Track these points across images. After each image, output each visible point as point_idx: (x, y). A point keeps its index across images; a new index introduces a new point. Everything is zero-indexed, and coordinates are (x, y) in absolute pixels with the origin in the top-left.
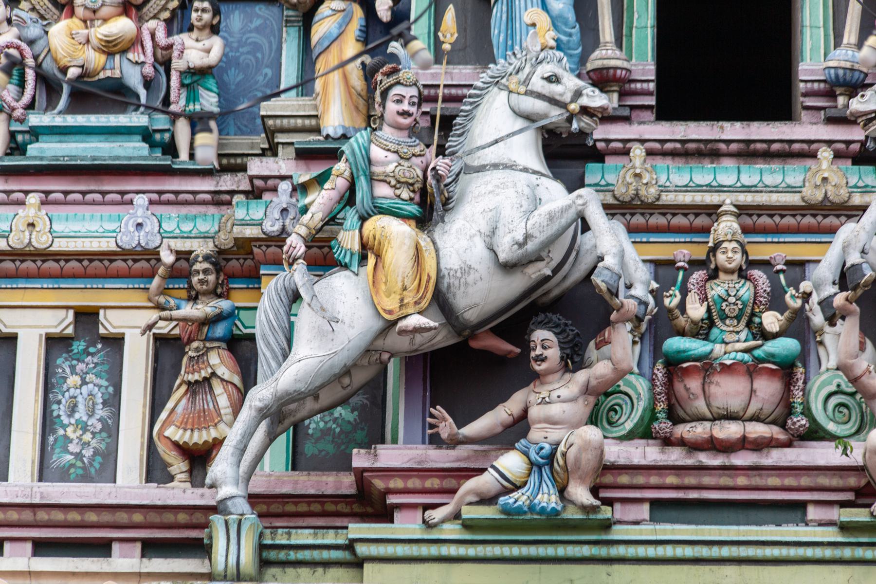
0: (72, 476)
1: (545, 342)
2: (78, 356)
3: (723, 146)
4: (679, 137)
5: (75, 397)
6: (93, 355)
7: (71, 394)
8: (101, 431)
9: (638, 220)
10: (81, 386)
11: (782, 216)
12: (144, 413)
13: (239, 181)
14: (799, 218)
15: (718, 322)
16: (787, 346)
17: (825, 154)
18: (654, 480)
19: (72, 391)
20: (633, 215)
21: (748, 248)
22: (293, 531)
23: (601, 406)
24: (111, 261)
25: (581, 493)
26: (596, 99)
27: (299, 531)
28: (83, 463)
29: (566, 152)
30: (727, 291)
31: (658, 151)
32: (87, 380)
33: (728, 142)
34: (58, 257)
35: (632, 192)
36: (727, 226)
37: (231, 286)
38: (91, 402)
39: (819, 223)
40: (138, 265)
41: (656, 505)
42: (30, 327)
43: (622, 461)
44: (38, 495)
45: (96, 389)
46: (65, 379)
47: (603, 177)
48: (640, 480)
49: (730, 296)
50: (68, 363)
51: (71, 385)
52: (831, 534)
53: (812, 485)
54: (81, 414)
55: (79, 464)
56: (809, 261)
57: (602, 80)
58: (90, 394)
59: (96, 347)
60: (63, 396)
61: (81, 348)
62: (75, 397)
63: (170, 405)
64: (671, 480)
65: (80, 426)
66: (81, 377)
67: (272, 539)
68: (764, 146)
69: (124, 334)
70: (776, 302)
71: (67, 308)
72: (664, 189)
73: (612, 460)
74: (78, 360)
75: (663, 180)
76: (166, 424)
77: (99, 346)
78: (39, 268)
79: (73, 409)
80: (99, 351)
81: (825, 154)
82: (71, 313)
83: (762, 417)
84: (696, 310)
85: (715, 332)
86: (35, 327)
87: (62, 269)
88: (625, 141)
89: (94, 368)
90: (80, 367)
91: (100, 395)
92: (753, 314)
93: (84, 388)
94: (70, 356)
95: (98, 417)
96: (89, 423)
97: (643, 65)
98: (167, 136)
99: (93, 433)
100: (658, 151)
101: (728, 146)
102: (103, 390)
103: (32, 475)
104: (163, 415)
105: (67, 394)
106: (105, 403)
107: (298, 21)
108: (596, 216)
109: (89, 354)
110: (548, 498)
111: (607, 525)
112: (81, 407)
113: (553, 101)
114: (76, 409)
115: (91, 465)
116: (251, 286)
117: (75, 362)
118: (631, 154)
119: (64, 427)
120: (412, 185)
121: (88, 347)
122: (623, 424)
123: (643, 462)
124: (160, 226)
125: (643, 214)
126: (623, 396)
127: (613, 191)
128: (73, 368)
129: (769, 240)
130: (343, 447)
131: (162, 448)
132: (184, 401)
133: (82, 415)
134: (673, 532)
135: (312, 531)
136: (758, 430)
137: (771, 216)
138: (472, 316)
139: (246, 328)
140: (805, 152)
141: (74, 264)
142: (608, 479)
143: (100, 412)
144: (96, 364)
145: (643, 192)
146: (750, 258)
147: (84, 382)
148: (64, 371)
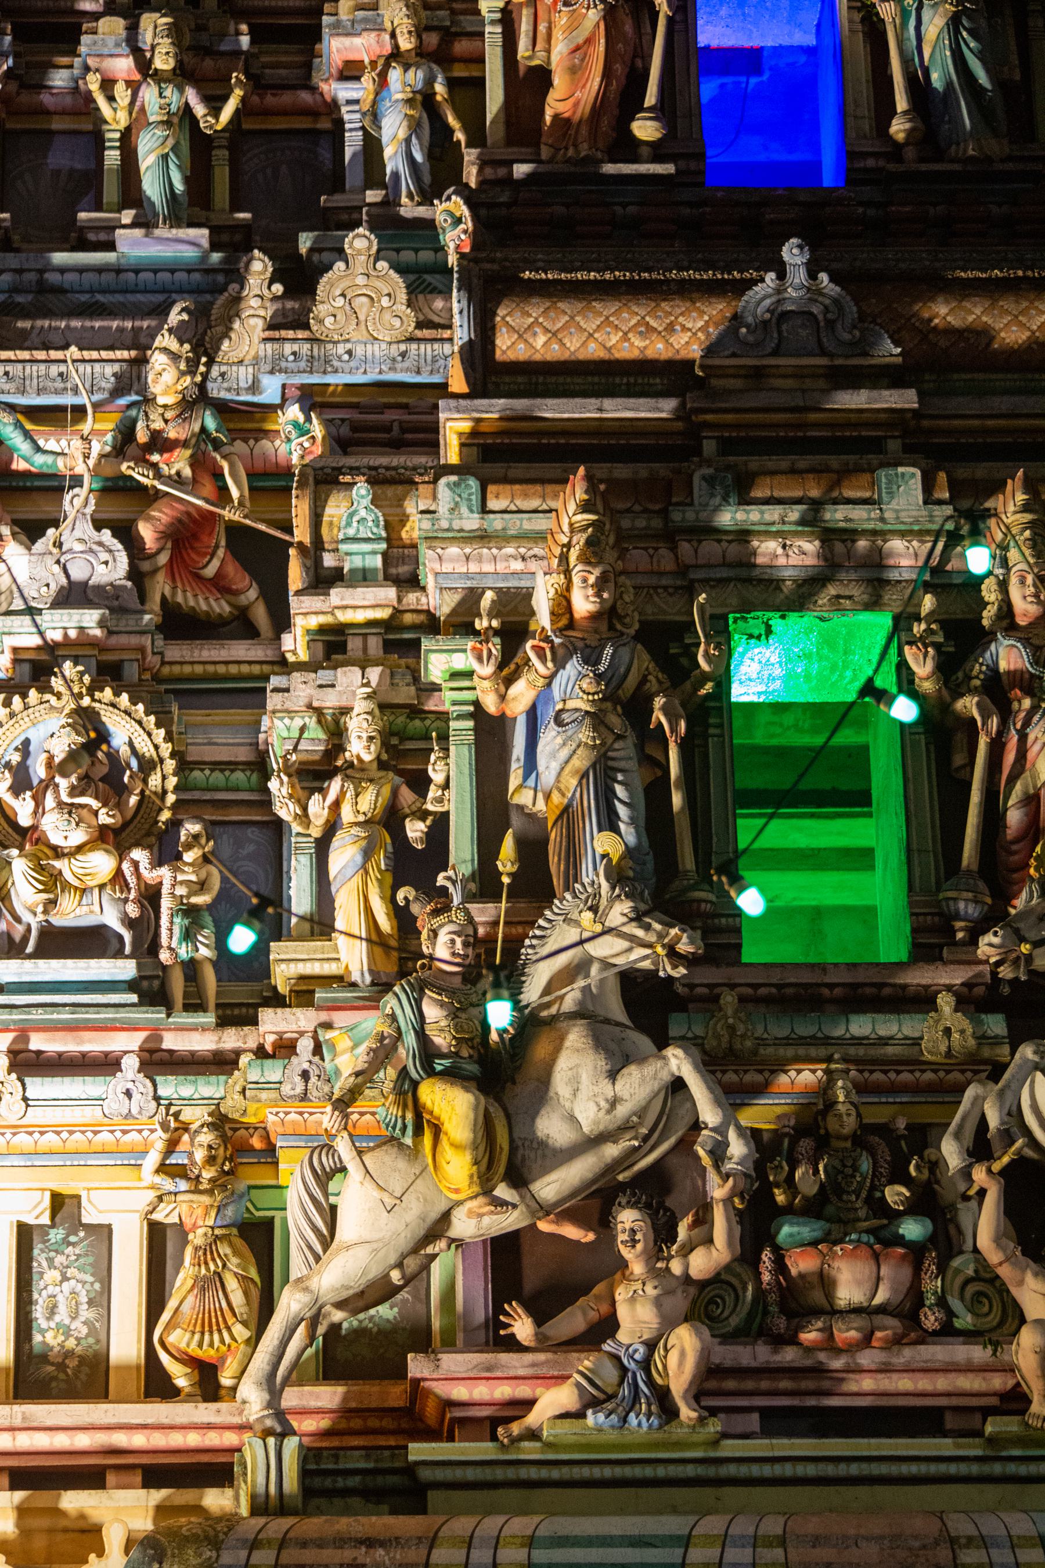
0: (54, 1392)
3: (826, 991)
4: (775, 981)
6: (74, 1244)
8: (87, 1336)
9: (731, 1077)
10: (61, 1282)
11: (898, 1072)
12: (140, 1314)
13: (245, 1036)
14: (917, 1074)
15: (834, 1199)
17: (945, 1002)
18: (765, 1385)
19: (50, 1289)
20: (724, 1072)
21: (862, 1109)
22: (342, 1453)
24: (95, 1133)
27: (349, 1453)
28: (67, 1375)
30: (842, 1161)
33: (831, 986)
35: (724, 1044)
37: (240, 1160)
39: (941, 1080)
40: (128, 1138)
41: (765, 1413)
43: (728, 1363)
44: (20, 1416)
45: (80, 1285)
46: (41, 1274)
47: (689, 1028)
48: (750, 1385)
49: (845, 1166)
50: (44, 1255)
53: (950, 1388)
54: (62, 1315)
55: (62, 1376)
56: (930, 1125)
58: (73, 1292)
61: (59, 1237)
63: (172, 1304)
64: (785, 1384)
67: (317, 1463)
68: (874, 990)
70: (899, 1176)
71: (43, 1190)
72: (761, 1042)
73: (717, 1361)
74: (57, 1251)
75: (759, 1031)
76: (170, 1326)
77: (82, 1234)
79: (52, 1311)
80: (82, 1240)
82: (48, 1194)
83: (890, 1309)
85: (830, 1210)
88: (711, 986)
90: (59, 1259)
91: (84, 1293)
92: (873, 1188)
93: (65, 1284)
95: (83, 1319)
96: (73, 1327)
98: (156, 983)
99: (77, 1339)
101: (831, 990)
102: (88, 1286)
103: (7, 1392)
104: (165, 1317)
105: (44, 1293)
106: (91, 1303)
107: (310, 848)
109: (69, 1244)
115: (77, 1378)
117: (52, 1254)
118: (722, 1002)
119: (43, 1332)
120: (471, 1039)
121: (68, 1236)
122: (727, 1318)
123: (754, 1364)
124: (155, 1090)
125: (736, 1072)
126: (725, 1286)
127: (703, 1044)
128: (50, 1261)
129: (884, 1100)
130: (382, 1351)
131: (164, 1357)
132: (190, 1299)
134: (792, 1447)
135: (363, 1452)
137: (885, 1072)
139: (258, 1210)
142: (712, 1384)
143: (86, 1313)
144: (79, 1256)
145: (738, 1046)
146: (865, 1121)
147: (65, 1278)
148: (40, 1265)
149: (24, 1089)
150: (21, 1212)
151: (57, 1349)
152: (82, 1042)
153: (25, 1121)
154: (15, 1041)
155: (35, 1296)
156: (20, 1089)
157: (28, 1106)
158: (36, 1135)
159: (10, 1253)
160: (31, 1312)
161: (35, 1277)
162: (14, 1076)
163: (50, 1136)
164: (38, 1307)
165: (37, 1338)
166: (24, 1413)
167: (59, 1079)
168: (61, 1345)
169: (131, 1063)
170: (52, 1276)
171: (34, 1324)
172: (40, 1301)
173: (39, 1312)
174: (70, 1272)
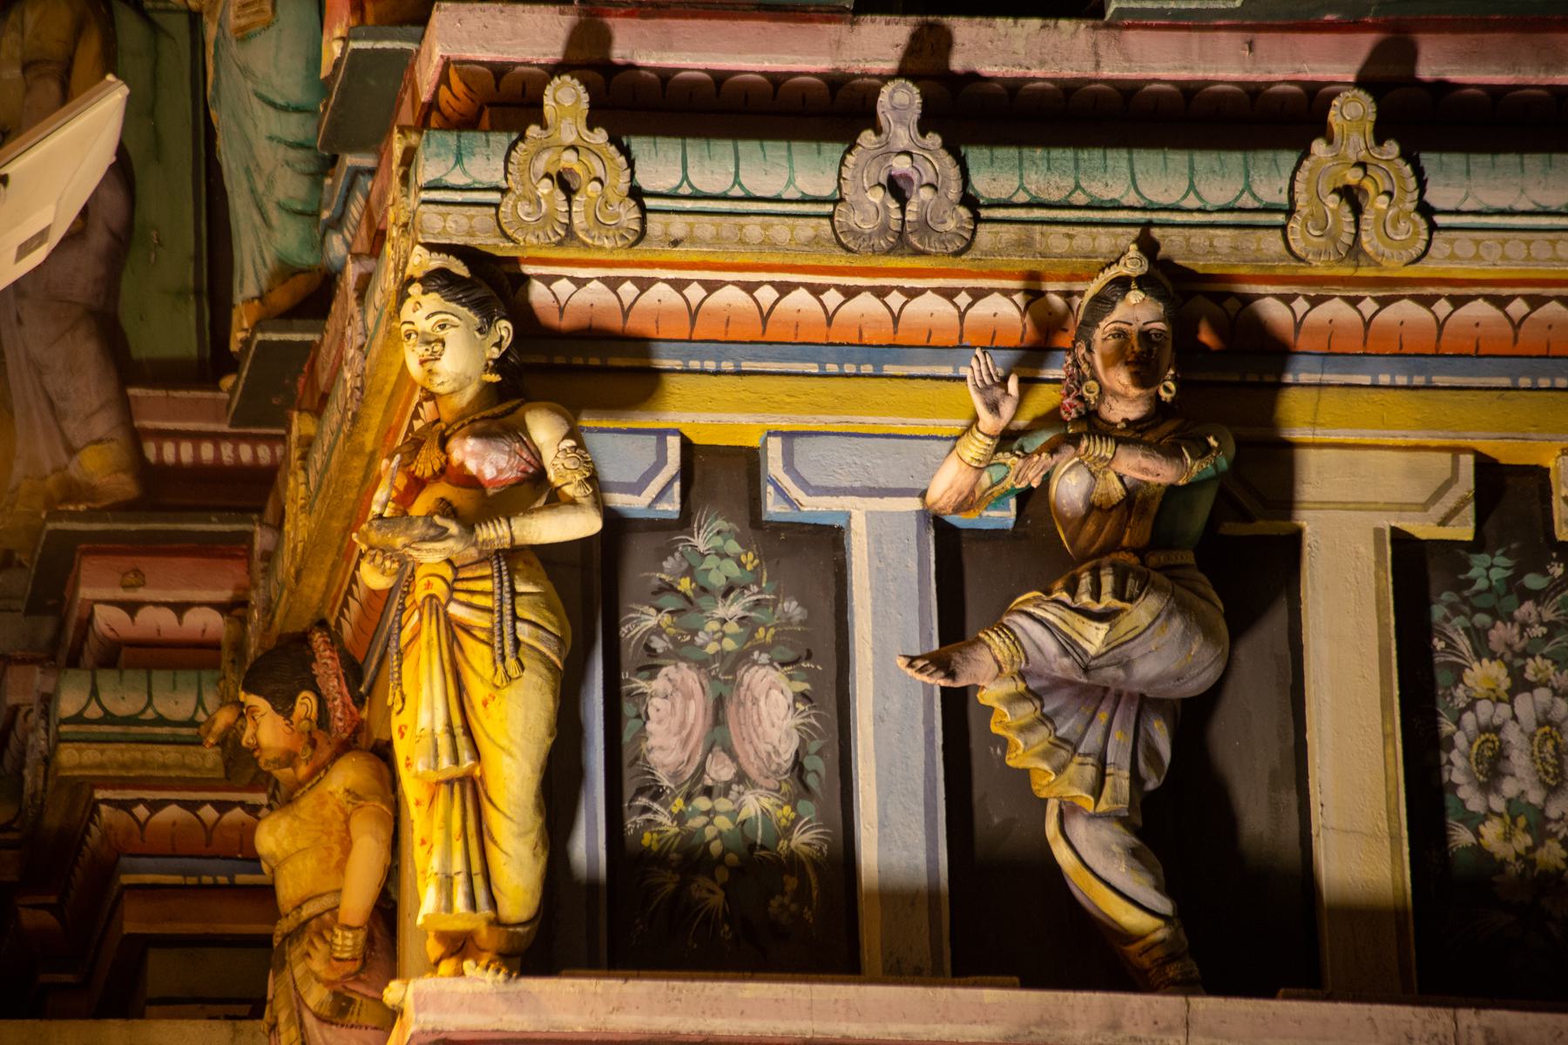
2: (1489, 601)
5: (1497, 730)
6: (1538, 597)
7: (1483, 719)
10: (1512, 693)
19: (1484, 708)
32: (1530, 674)
34: (1429, 290)
38: (1550, 745)
42: (1344, 505)
46: (1458, 671)
50: (1459, 621)
51: (1480, 691)
54: (1522, 780)
58: (1544, 720)
59: (1546, 573)
60: (1458, 723)
61: (1496, 574)
62: (1497, 730)
65: (1522, 822)
66: (1509, 665)
69: (849, 516)
71: (1456, 451)
74: (1494, 613)
78: (896, 319)
79: (1493, 768)
82: (1467, 461)
86: (1361, 506)
87: (1441, 325)
89: (1548, 637)
90: (1501, 633)
93: (1523, 703)
94: (1465, 600)
96: (1553, 811)
105: (1468, 718)
109: (1525, 595)
112: (1519, 760)
114: (1502, 765)
116: (1544, 382)
117: (1482, 619)
119: (1474, 821)
121: (1519, 572)
133: (1526, 786)
141: (1406, 311)
147: (1520, 685)
148: (1451, 646)
149: (1422, 185)
150: (1402, 507)
151: (1515, 868)
152: (668, 47)
153: (1427, 269)
154: (1377, 55)
155: (1447, 727)
156: (1412, 183)
157: (1433, 228)
158: (1443, 308)
159: (1380, 612)
160: (1438, 768)
161: (1442, 677)
162: (1392, 148)
163: (1480, 310)
164: (1455, 756)
165: (1462, 837)
166: (1489, 1032)
167: (1511, 159)
168: (1526, 858)
169: (1352, 113)
170: (1485, 674)
171: (1450, 801)
172: (1460, 740)
173: (1458, 769)
174: (1534, 668)
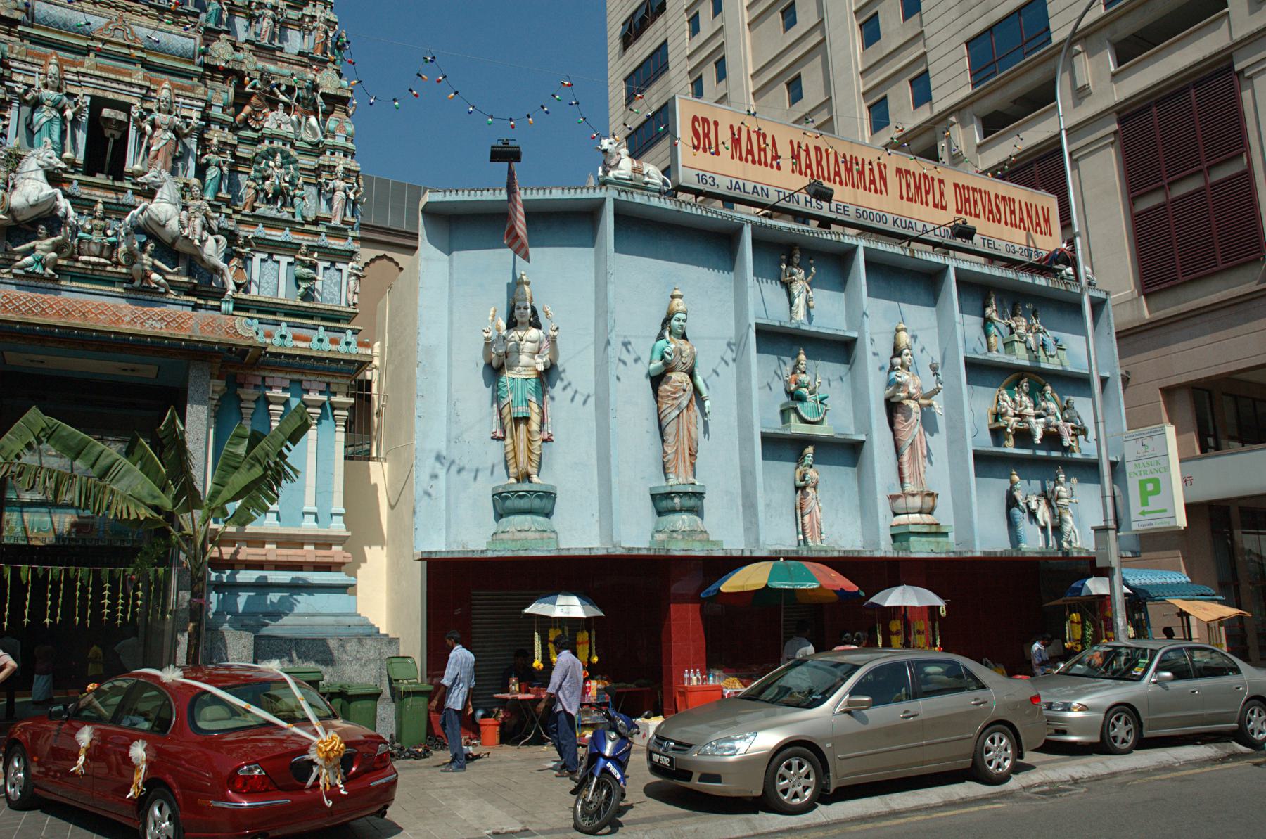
1: (42, 229)
16: (113, 239)
17: (130, 192)
23: (57, 248)
25: (49, 271)
26: (64, 166)
29: (53, 178)
31: (81, 183)
36: (100, 206)
52: (121, 290)
57: (67, 161)
81: (130, 192)
84: (88, 227)
97: (80, 158)
100: (81, 183)
108: (60, 196)
110: (39, 270)
111: (57, 280)
113: (50, 164)
136: (102, 260)
138: (20, 218)
140: (124, 191)
